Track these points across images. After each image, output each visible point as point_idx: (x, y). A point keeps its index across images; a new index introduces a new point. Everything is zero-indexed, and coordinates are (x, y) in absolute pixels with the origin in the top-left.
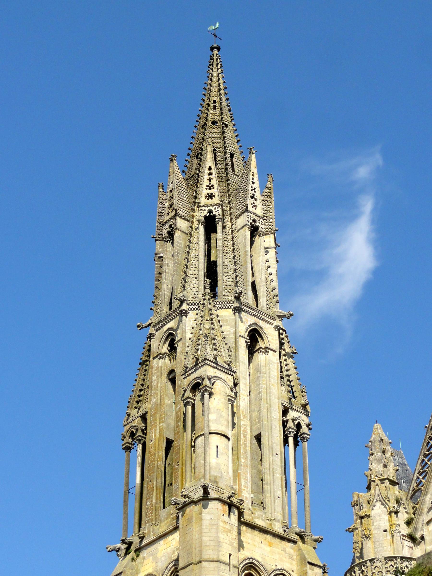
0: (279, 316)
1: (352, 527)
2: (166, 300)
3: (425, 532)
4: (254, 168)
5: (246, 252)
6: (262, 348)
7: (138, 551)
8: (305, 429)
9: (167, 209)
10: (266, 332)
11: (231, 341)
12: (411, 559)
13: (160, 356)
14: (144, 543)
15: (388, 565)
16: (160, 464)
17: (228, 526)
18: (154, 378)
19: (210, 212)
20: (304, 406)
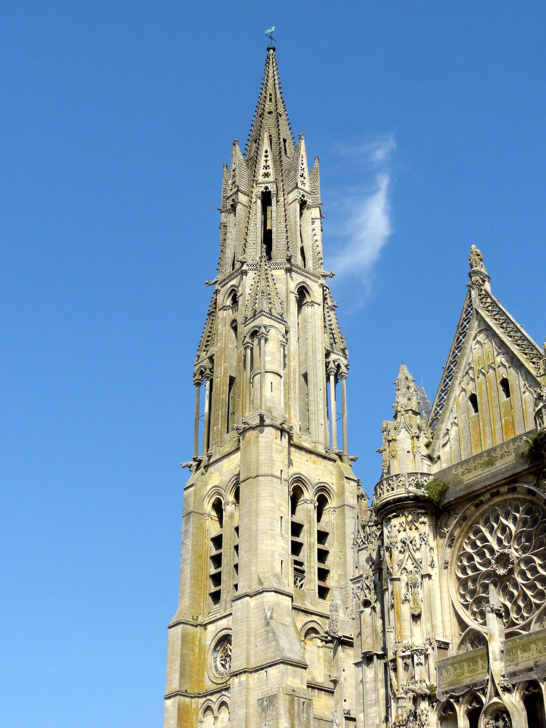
0: (324, 276)
1: (381, 449)
2: (230, 261)
3: (441, 453)
4: (303, 152)
5: (296, 222)
6: (309, 302)
7: (207, 467)
8: (343, 369)
9: (230, 186)
10: (312, 289)
11: (283, 297)
12: (429, 475)
13: (224, 308)
14: (211, 461)
15: (410, 480)
16: (225, 396)
17: (280, 448)
18: (220, 326)
19: (266, 188)
20: (343, 350)
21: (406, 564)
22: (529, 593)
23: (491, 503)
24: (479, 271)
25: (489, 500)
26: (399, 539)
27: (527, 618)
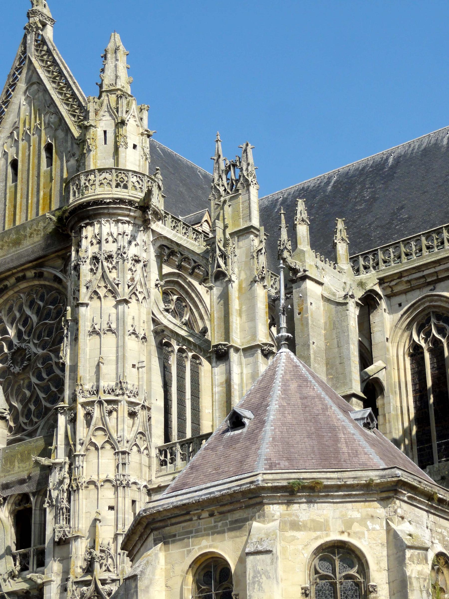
22: (42, 395)
23: (16, 289)
24: (39, 11)
25: (14, 286)
27: (36, 423)
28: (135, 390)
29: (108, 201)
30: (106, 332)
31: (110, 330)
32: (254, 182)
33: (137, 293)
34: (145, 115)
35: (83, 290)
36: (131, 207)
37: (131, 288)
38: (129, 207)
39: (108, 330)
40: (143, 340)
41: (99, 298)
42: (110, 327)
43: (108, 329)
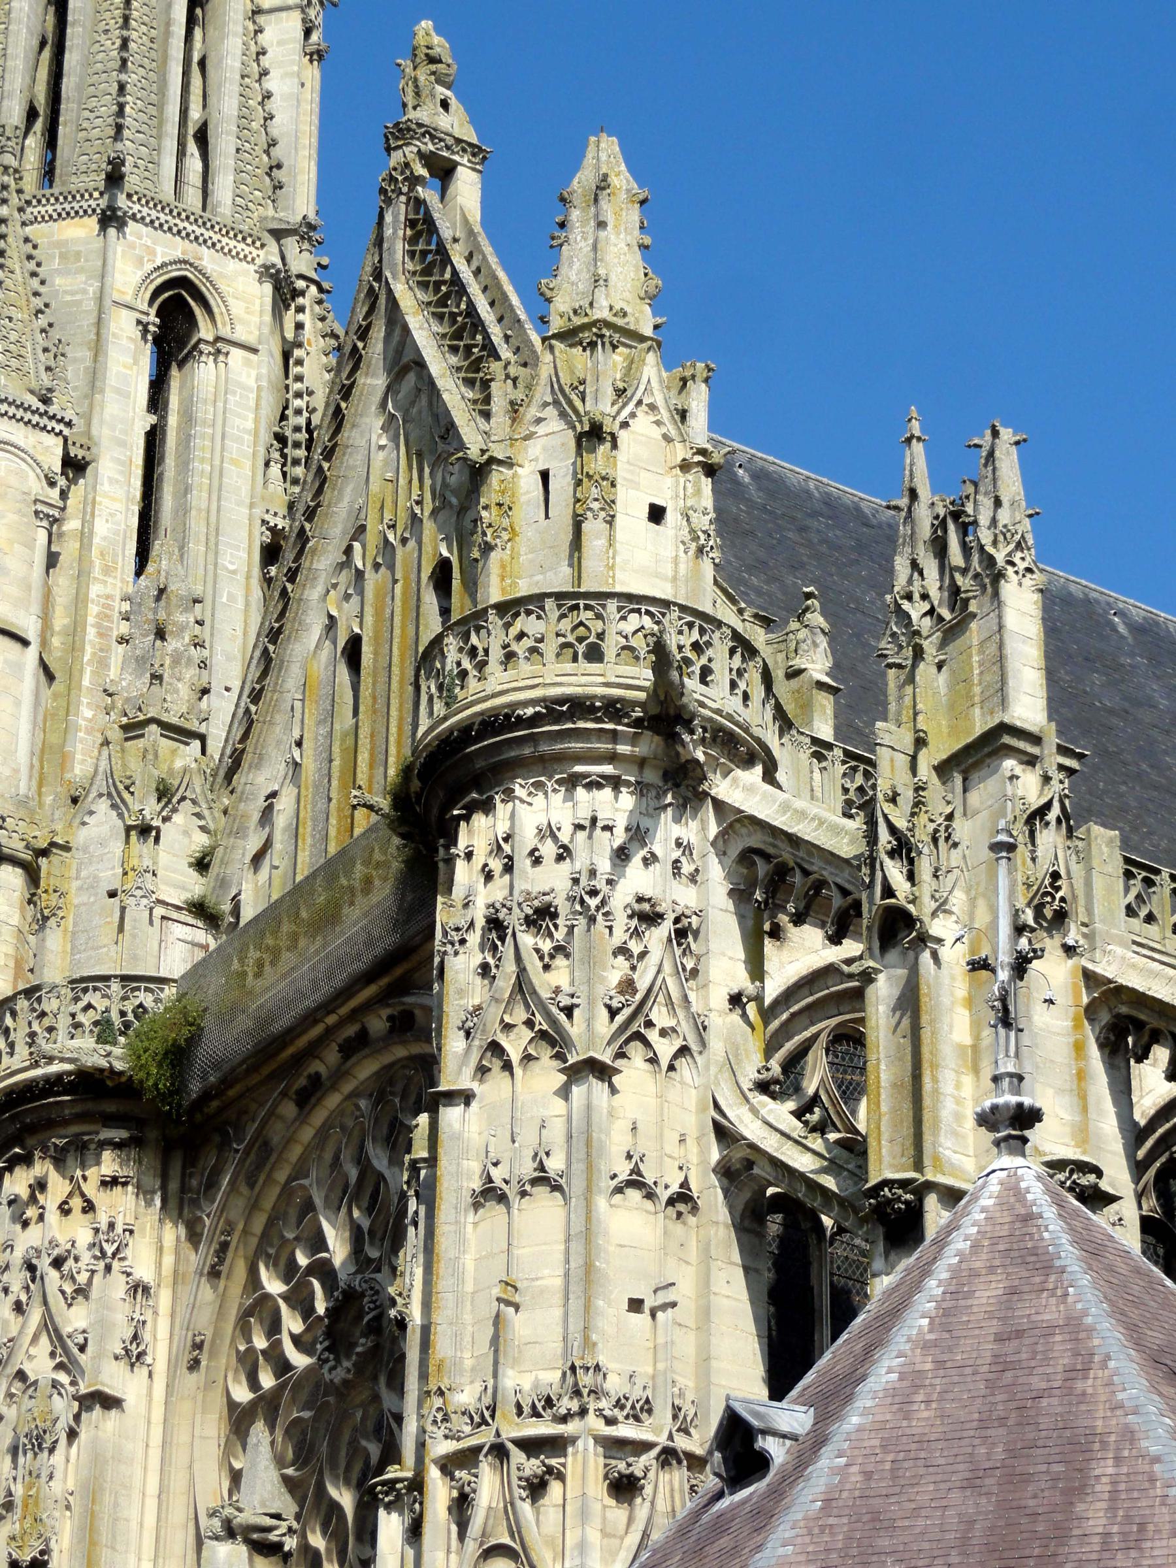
6: (207, 342)
10: (223, 287)
21: (30, 1357)
23: (348, 1087)
24: (420, 125)
25: (339, 1075)
26: (18, 1254)
28: (637, 1393)
29: (530, 711)
30: (528, 1187)
31: (542, 1179)
32: (1022, 566)
33: (653, 1036)
34: (698, 400)
35: (454, 1045)
36: (619, 723)
37: (620, 1019)
38: (610, 726)
39: (535, 1182)
40: (681, 1207)
41: (508, 1066)
42: (542, 1168)
43: (536, 1174)
